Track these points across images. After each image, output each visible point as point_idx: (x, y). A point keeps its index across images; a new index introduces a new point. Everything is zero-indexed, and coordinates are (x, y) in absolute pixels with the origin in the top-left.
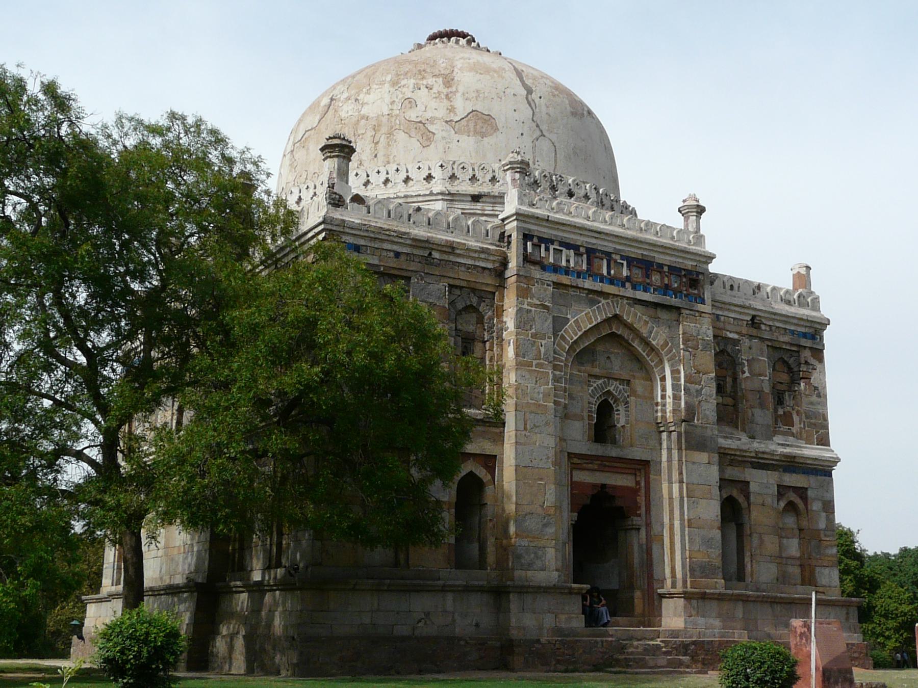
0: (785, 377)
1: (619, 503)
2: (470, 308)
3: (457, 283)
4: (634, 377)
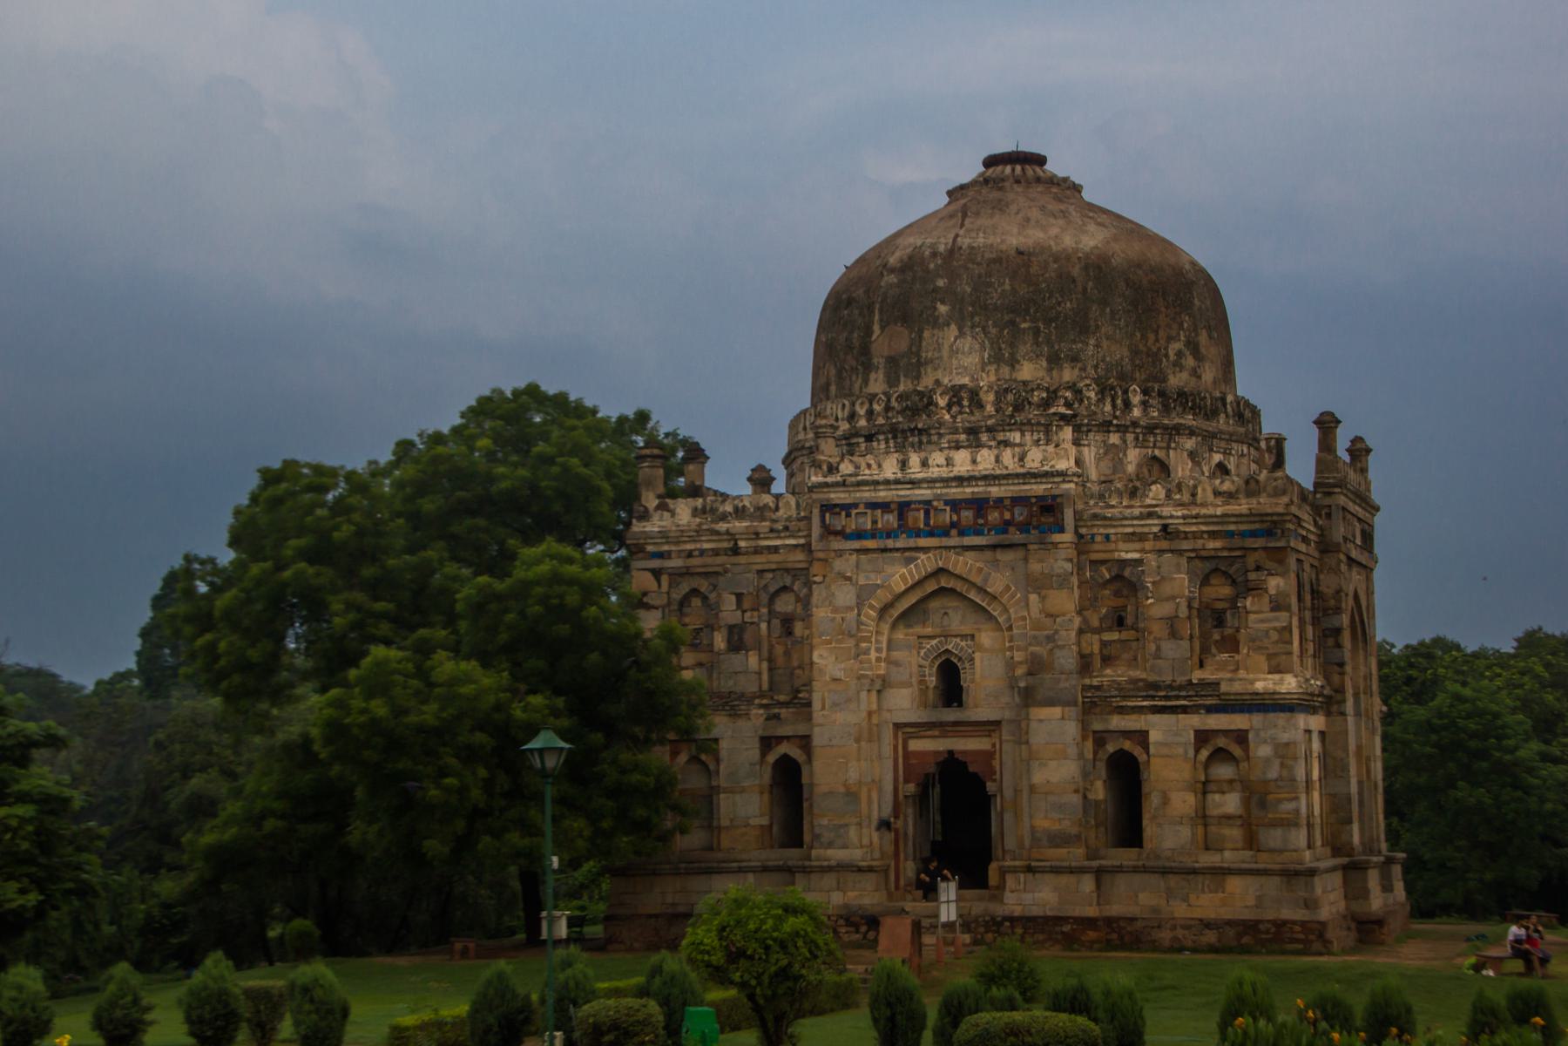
0: (1226, 591)
1: (971, 769)
2: (784, 589)
3: (766, 567)
4: (979, 630)
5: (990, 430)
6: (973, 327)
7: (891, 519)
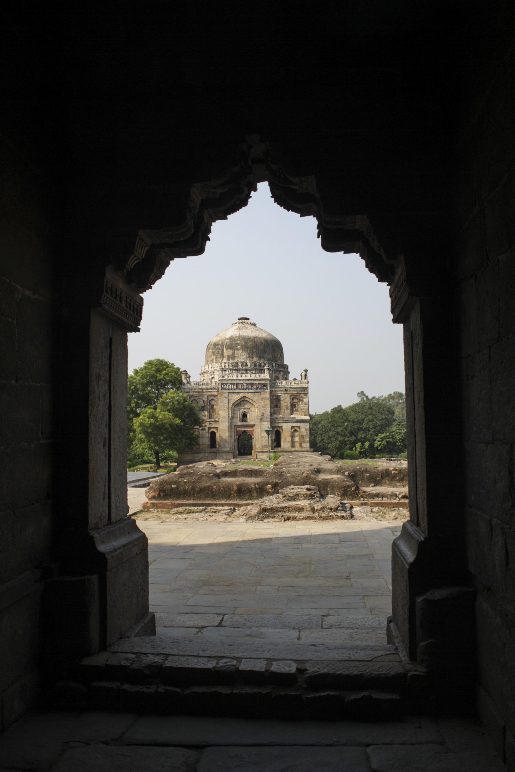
2: (212, 399)
5: (250, 370)
7: (235, 387)
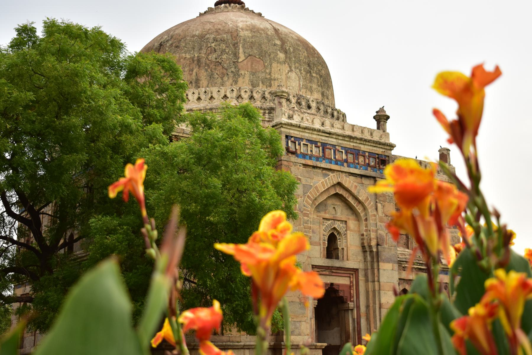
1: (341, 294)
4: (349, 219)
6: (295, 68)
